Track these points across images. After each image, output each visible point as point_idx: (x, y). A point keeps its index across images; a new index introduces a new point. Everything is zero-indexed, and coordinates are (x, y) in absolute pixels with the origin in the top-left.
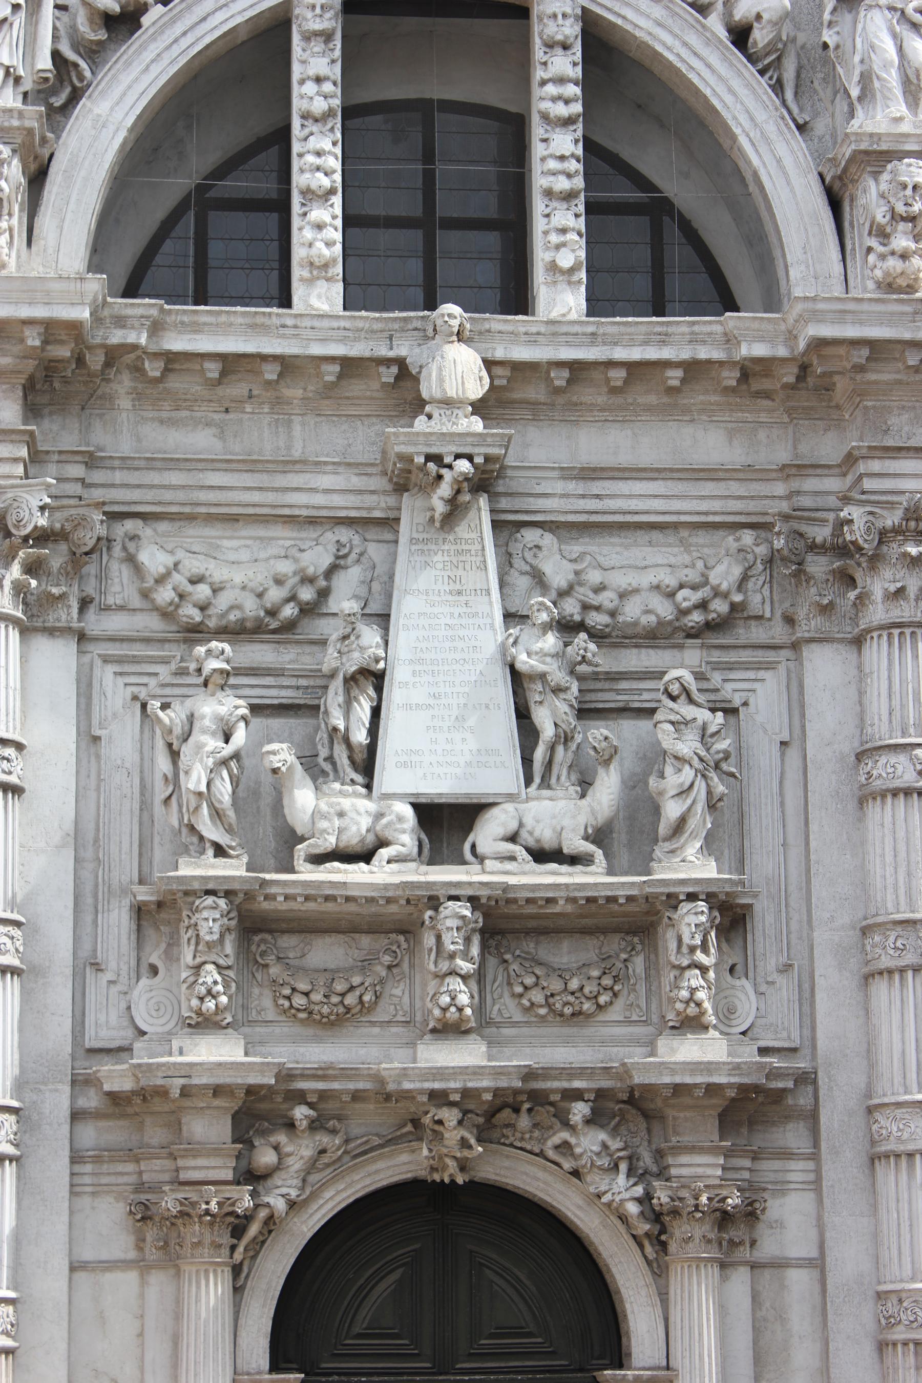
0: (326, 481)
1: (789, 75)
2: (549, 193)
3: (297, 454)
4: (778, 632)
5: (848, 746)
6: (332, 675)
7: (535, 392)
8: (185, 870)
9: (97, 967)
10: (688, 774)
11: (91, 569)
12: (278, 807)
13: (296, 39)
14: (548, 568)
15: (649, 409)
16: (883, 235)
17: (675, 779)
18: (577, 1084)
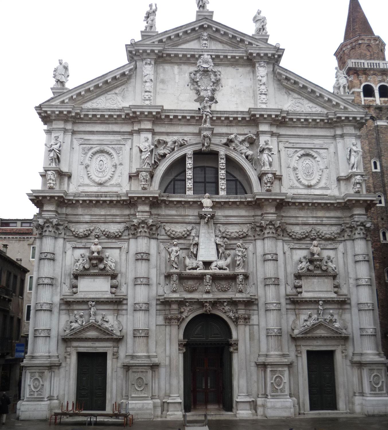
0: (190, 218)
1: (254, 162)
2: (221, 178)
3: (187, 214)
4: (253, 238)
5: (262, 253)
6: (191, 244)
7: (219, 205)
8: (171, 271)
9: (160, 284)
10: (240, 258)
11: (159, 230)
12: (184, 262)
13: (187, 158)
14: (221, 229)
15: (235, 208)
16: (266, 184)
17: (238, 258)
18: (225, 300)
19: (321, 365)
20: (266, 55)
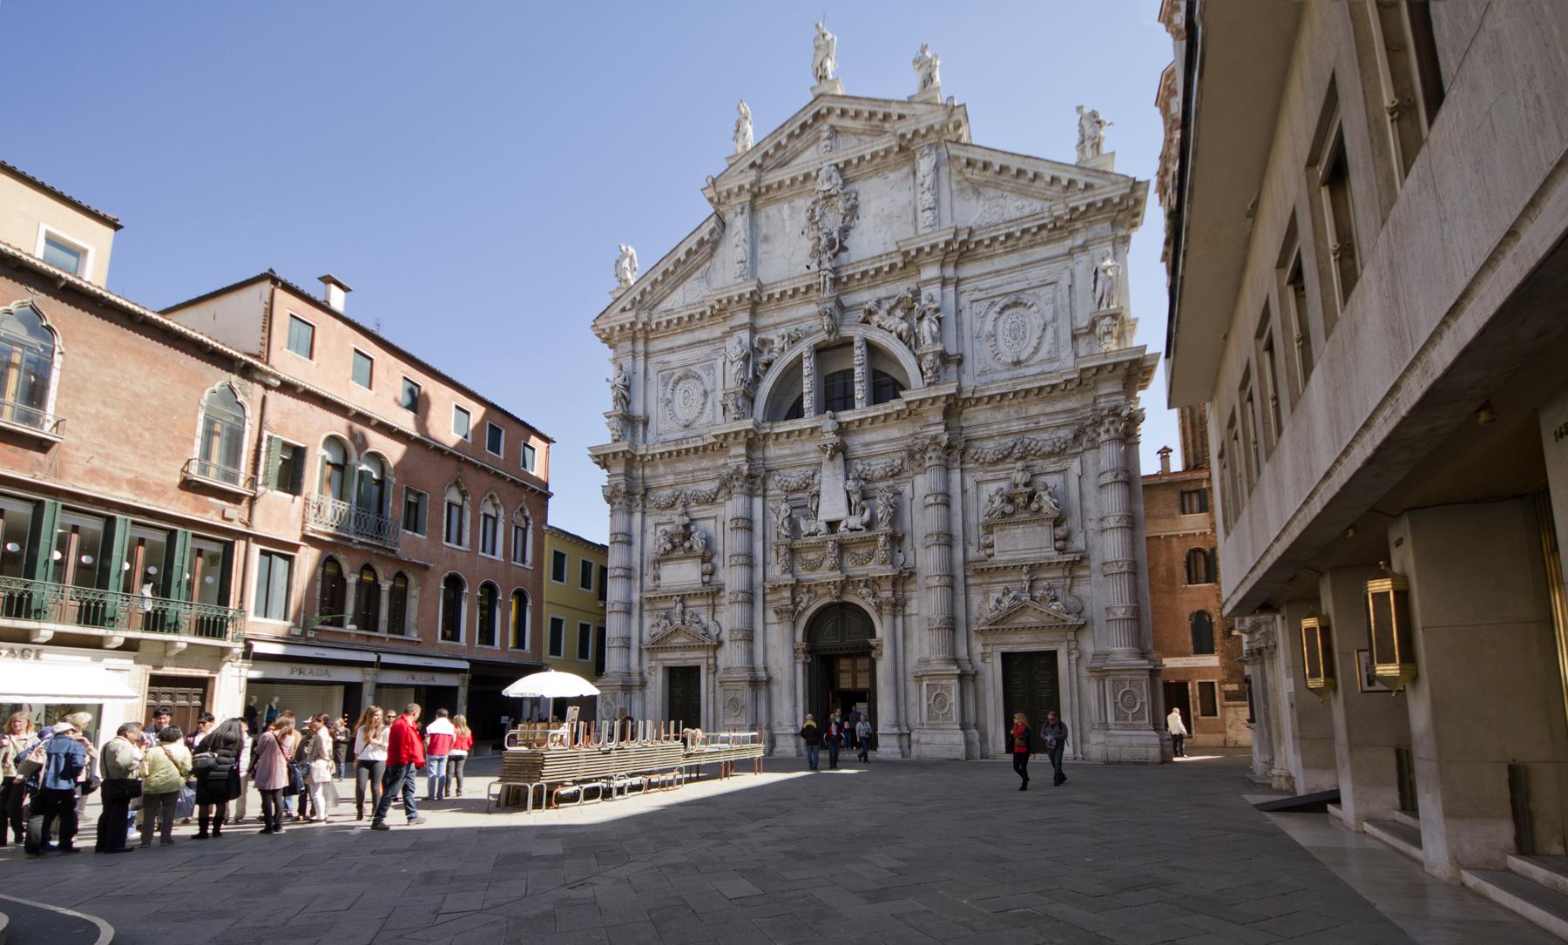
19: (1030, 680)
20: (930, 128)
